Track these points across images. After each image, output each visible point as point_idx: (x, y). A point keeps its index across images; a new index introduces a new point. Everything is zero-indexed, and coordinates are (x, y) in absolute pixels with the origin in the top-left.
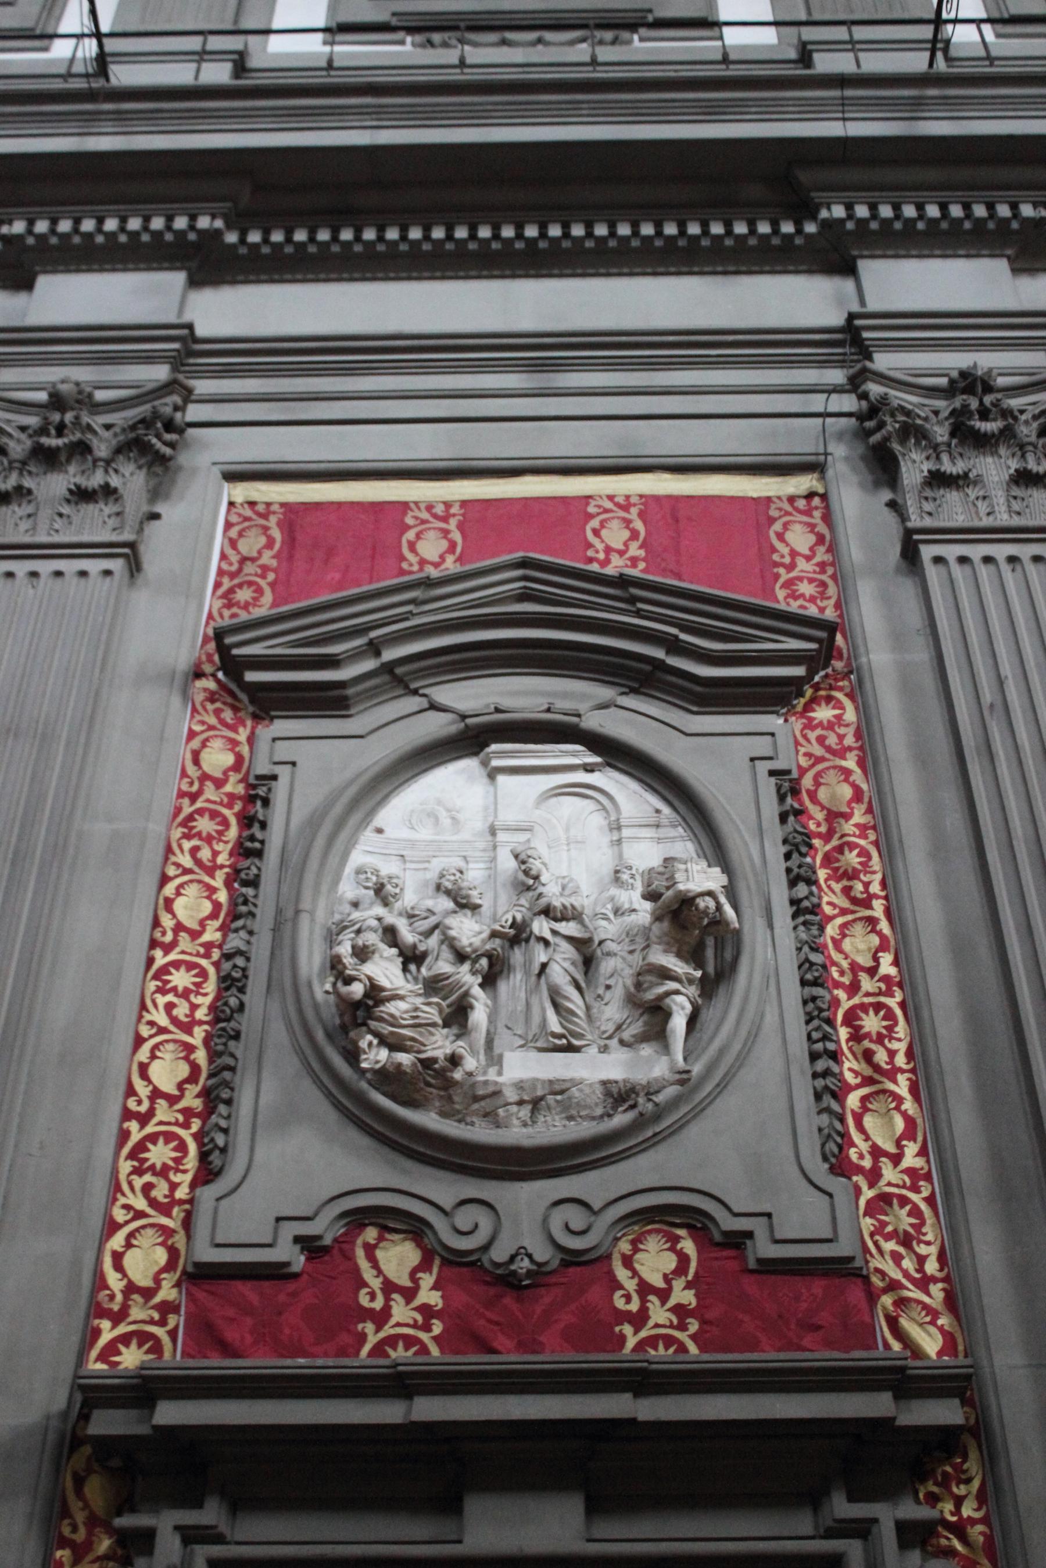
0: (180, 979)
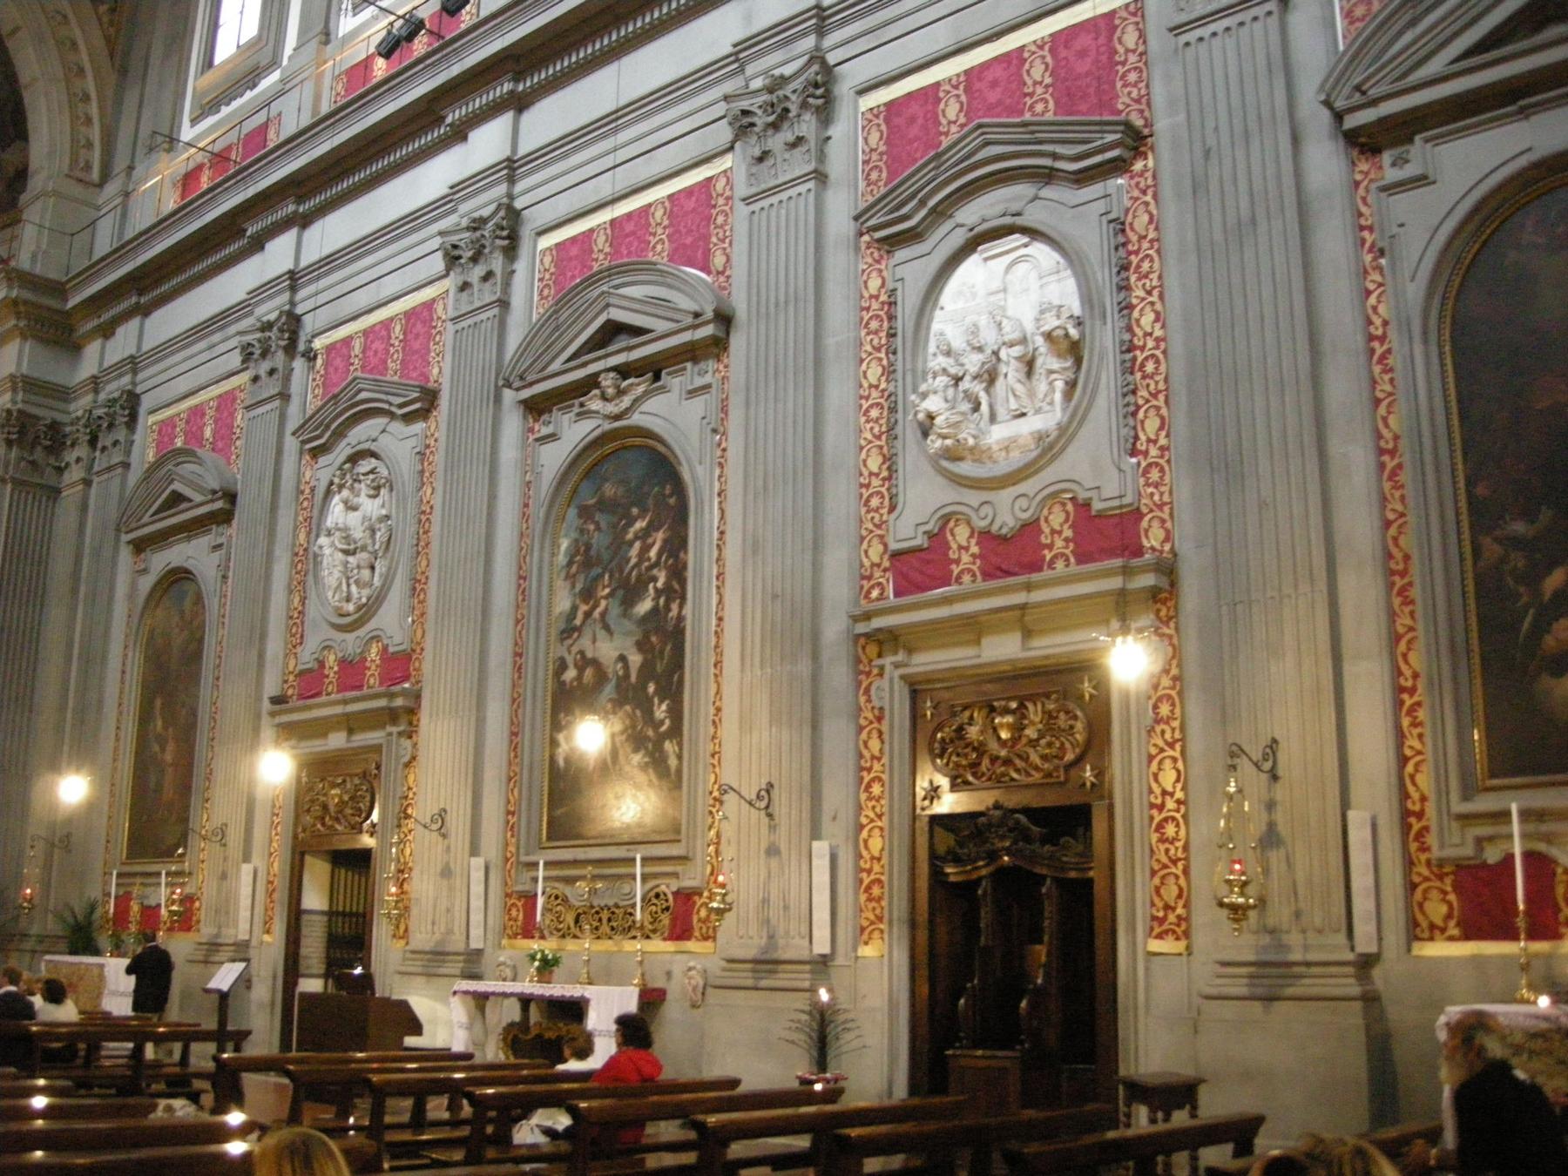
0: (874, 413)
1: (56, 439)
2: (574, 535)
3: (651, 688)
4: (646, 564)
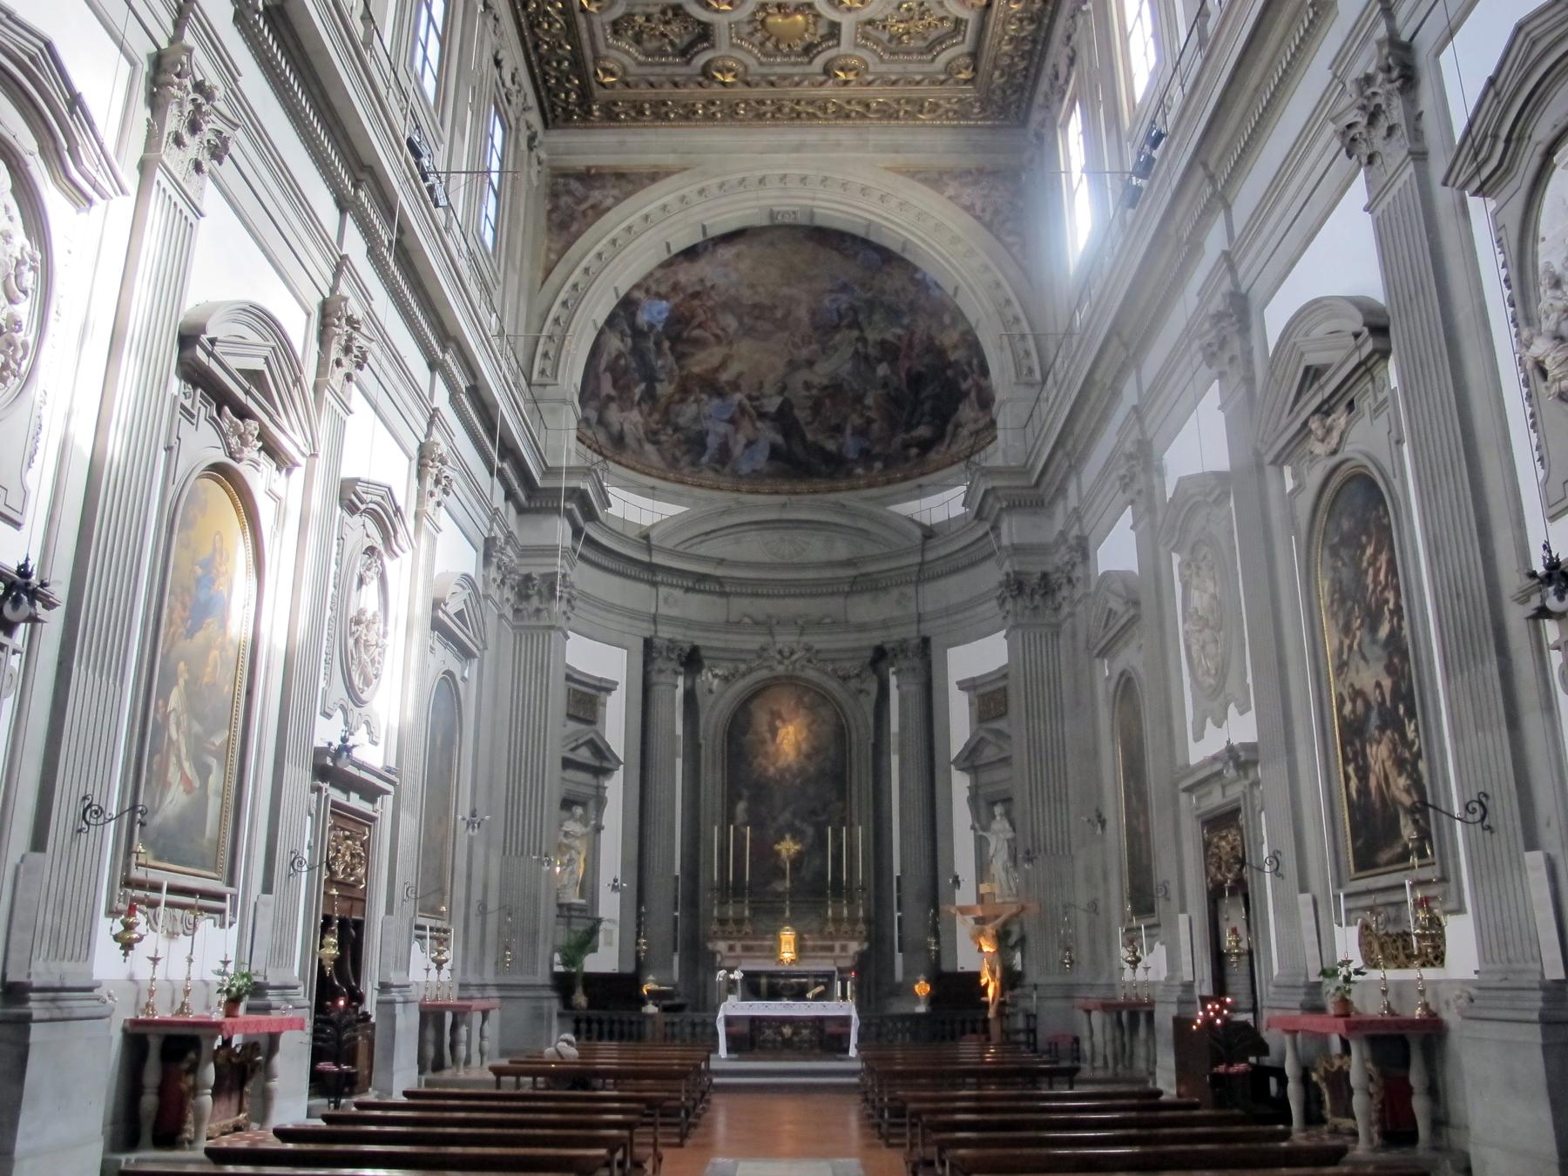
1: (1047, 586)
2: (1330, 574)
3: (1401, 710)
4: (1379, 588)
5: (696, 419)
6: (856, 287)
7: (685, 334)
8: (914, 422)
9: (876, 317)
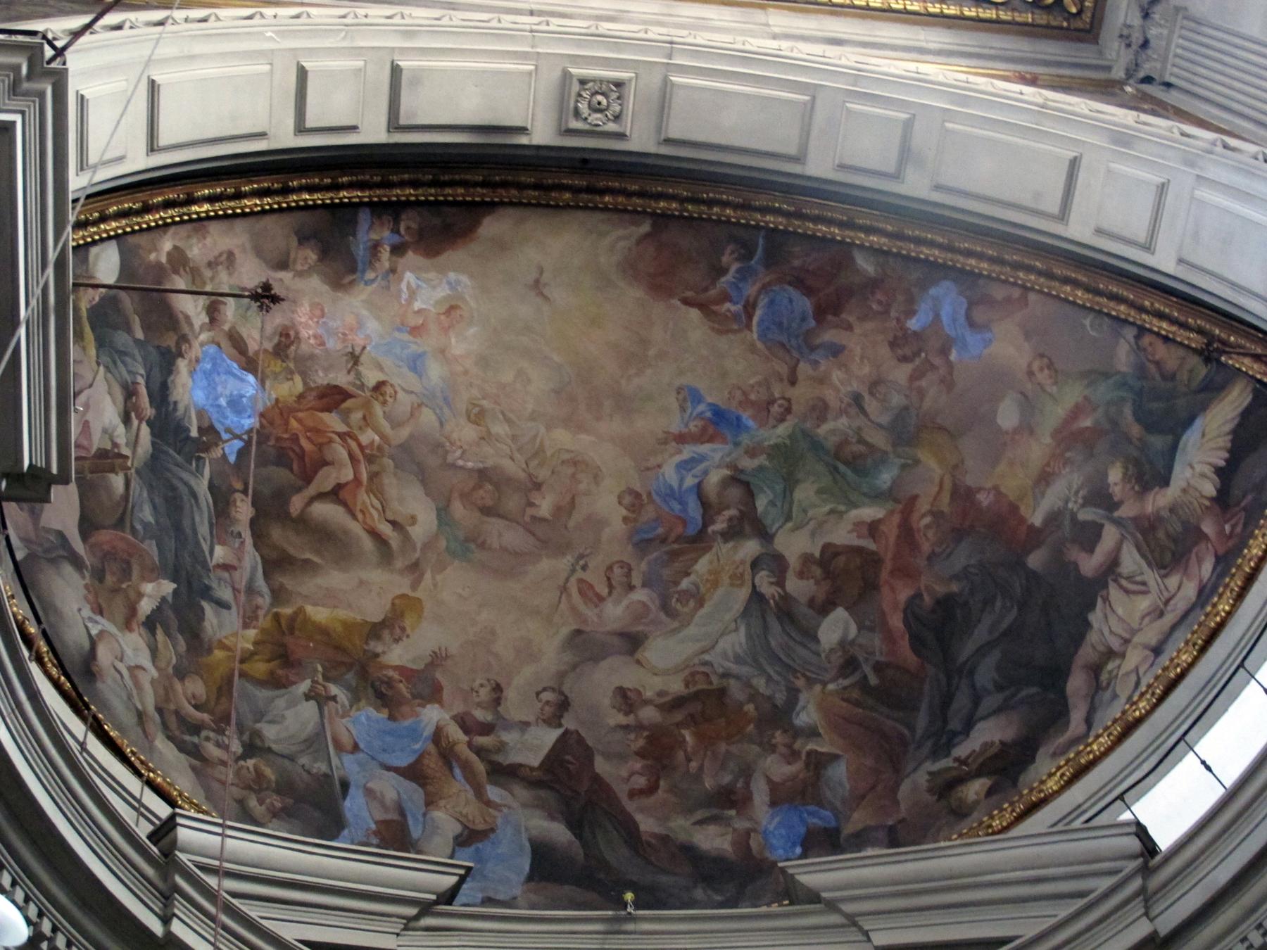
5: (315, 743)
6: (747, 418)
7: (296, 504)
8: (955, 724)
9: (805, 493)
